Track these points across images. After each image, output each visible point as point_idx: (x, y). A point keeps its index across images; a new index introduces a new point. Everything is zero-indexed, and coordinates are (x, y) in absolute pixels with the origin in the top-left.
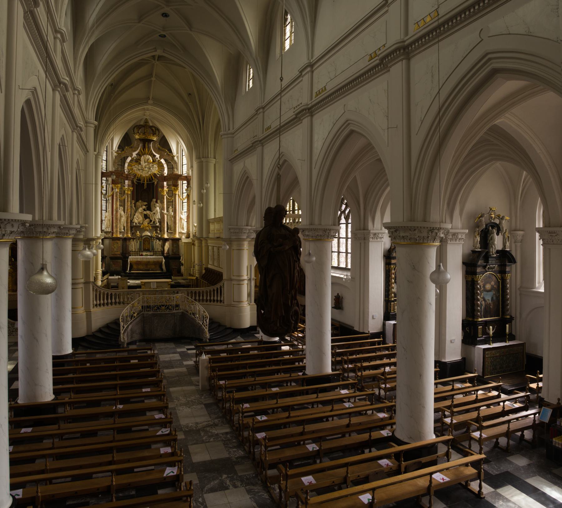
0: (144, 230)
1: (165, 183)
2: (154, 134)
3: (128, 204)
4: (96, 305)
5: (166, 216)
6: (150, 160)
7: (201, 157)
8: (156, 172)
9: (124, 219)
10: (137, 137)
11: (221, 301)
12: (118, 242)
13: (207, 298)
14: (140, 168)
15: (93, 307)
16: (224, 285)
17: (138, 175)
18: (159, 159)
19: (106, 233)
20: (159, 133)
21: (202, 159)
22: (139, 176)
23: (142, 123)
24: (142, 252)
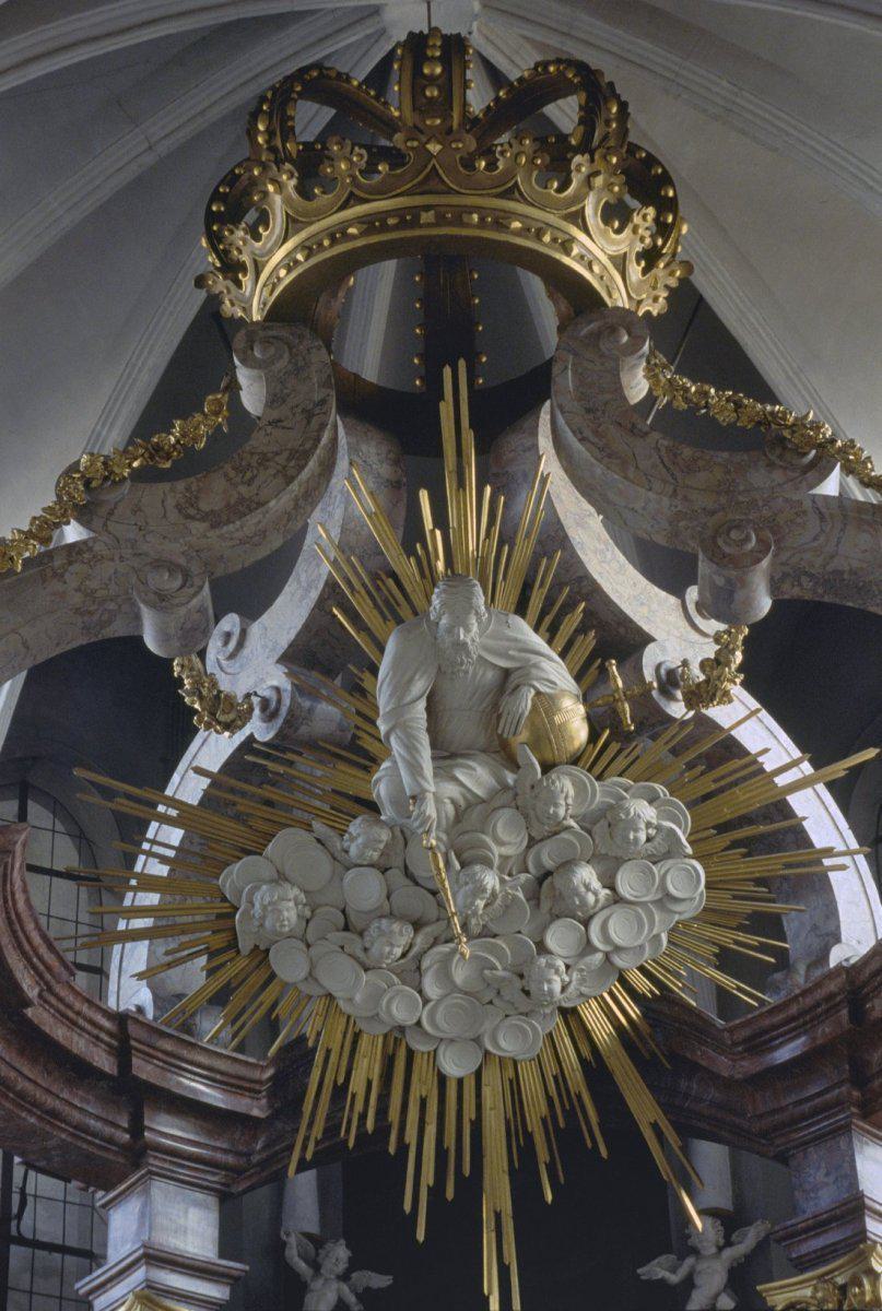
6: (546, 704)
14: (366, 890)
17: (334, 1039)
22: (367, 1068)
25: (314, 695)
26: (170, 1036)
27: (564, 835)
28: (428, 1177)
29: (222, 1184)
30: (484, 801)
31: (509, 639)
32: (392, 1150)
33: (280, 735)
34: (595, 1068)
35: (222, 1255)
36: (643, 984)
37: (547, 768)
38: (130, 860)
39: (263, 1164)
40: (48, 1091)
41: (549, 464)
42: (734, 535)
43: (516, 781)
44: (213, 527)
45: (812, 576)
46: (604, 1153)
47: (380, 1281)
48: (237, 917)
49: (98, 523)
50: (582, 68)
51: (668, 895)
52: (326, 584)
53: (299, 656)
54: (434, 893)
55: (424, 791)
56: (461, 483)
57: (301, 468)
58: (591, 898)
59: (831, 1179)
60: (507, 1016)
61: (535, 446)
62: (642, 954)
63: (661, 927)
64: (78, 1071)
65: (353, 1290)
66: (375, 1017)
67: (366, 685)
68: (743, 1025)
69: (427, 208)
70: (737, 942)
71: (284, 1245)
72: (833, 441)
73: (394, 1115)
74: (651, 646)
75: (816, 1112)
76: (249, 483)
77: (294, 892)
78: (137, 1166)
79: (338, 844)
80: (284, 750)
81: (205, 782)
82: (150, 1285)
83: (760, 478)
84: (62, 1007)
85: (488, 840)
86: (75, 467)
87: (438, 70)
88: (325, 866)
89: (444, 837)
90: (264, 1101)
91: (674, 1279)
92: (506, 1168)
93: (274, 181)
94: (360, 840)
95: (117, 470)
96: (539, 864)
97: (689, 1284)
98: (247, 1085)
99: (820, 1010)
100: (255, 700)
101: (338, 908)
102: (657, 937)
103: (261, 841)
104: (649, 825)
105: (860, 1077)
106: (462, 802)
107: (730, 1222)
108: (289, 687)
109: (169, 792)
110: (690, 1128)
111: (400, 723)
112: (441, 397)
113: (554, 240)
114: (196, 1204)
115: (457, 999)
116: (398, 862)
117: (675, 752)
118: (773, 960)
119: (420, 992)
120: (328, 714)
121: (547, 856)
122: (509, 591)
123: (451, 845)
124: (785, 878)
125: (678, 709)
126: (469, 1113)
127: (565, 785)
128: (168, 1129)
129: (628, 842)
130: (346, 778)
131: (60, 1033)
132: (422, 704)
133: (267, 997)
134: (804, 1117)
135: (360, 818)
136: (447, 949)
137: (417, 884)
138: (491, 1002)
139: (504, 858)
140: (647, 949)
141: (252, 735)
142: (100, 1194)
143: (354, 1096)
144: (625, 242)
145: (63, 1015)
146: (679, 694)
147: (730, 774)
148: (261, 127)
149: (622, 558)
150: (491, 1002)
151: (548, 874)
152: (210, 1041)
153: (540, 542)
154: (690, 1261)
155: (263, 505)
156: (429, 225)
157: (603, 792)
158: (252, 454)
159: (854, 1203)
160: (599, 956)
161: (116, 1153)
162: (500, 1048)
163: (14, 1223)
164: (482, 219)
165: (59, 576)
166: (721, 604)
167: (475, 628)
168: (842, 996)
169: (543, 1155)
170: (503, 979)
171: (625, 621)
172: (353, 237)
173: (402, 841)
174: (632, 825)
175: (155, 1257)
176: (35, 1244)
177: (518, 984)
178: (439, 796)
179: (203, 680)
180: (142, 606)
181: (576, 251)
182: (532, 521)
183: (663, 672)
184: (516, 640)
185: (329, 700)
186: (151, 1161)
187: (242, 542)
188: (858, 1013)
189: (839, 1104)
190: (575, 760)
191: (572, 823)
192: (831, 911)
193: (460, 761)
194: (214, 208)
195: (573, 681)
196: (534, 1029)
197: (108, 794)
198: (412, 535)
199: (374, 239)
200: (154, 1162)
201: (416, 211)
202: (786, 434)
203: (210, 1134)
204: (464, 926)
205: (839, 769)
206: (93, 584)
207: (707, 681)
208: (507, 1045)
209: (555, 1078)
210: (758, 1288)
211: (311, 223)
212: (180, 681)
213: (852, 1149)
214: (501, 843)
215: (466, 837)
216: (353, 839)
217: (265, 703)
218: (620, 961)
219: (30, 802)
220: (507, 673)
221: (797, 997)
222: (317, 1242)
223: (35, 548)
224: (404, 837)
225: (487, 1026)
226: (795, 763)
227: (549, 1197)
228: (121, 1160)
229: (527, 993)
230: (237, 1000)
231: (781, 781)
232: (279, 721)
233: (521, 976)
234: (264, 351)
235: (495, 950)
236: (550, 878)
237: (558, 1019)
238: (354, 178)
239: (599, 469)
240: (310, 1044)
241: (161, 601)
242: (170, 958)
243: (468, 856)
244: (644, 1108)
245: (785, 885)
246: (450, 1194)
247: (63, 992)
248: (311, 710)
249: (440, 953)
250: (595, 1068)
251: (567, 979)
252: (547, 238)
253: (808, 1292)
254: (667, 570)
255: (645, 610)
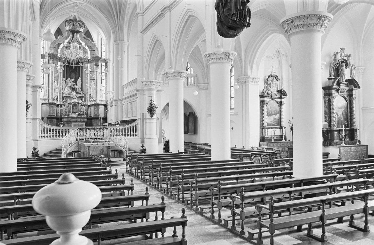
0: (72, 98)
2: (81, 26)
3: (60, 80)
4: (41, 137)
5: (89, 89)
7: (118, 40)
8: (82, 57)
9: (57, 90)
10: (68, 28)
11: (136, 135)
12: (53, 106)
13: (125, 134)
14: (70, 53)
15: (39, 138)
16: (138, 123)
18: (84, 46)
19: (44, 99)
20: (85, 26)
21: (119, 42)
22: (69, 59)
23: (72, 18)
24: (71, 114)
120: (69, 45)
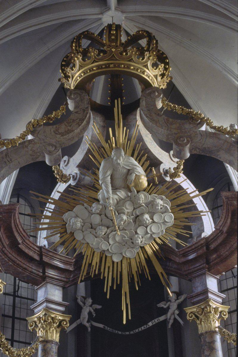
1: (212, 283)
6: (138, 177)
14: (96, 219)
17: (89, 253)
22: (96, 260)
25: (85, 175)
26: (52, 252)
27: (142, 207)
28: (110, 284)
29: (63, 285)
30: (123, 199)
31: (130, 162)
32: (102, 278)
33: (77, 184)
34: (148, 260)
35: (63, 301)
36: (159, 241)
37: (138, 192)
38: (42, 212)
39: (73, 281)
40: (24, 264)
41: (139, 122)
42: (181, 139)
43: (131, 195)
44: (62, 136)
45: (199, 149)
46: (150, 279)
47: (99, 307)
48: (67, 225)
49: (35, 135)
50: (147, 32)
51: (165, 221)
52: (88, 149)
53: (81, 166)
54: (112, 220)
55: (110, 197)
56: (119, 127)
57: (82, 123)
58: (148, 222)
59: (201, 285)
60: (128, 248)
61: (136, 118)
62: (159, 234)
63: (163, 228)
64: (31, 259)
65: (93, 309)
66: (98, 248)
67: (97, 173)
68: (182, 251)
69: (112, 64)
70: (181, 232)
71: (77, 299)
72: (204, 118)
73: (102, 270)
74: (162, 164)
75: (198, 270)
76: (70, 126)
77: (80, 220)
78: (44, 281)
79: (90, 209)
80: (78, 187)
81: (60, 194)
82: (47, 307)
83: (187, 126)
84: (27, 245)
85: (124, 208)
86: (30, 122)
87: (114, 32)
88: (87, 214)
89: (114, 207)
90: (73, 267)
91: (165, 307)
92: (128, 282)
93: (77, 57)
94: (95, 208)
95: (40, 123)
96: (136, 214)
97: (168, 308)
98: (69, 263)
99: (199, 247)
100: (71, 176)
101: (89, 223)
102: (163, 230)
103: (72, 208)
104: (161, 205)
105: (208, 262)
106: (118, 200)
107: (178, 294)
108: (79, 173)
109: (51, 196)
110: (169, 274)
111: (104, 181)
112: (114, 106)
113: (141, 71)
114: (58, 290)
115: (117, 244)
116: (104, 213)
117: (167, 188)
118: (189, 236)
119: (108, 243)
120: (88, 179)
121: (138, 212)
122: (130, 151)
123: (116, 209)
124: (192, 217)
125: (168, 179)
126: (119, 270)
127: (142, 196)
128: (51, 273)
129: (156, 208)
130: (92, 194)
131: (26, 251)
132: (109, 177)
133: (74, 243)
134: (195, 271)
135: (95, 204)
136: (115, 233)
137: (108, 218)
138: (124, 245)
139: (128, 212)
140: (160, 233)
141: (70, 184)
142: (36, 287)
143: (93, 266)
144: (157, 72)
145: (28, 247)
146: (168, 175)
147: (180, 194)
148: (74, 45)
149: (156, 144)
150: (124, 245)
151: (138, 216)
152: (60, 253)
153: (137, 140)
154: (169, 303)
155: (73, 131)
156: (112, 67)
157: (151, 198)
158: (71, 119)
159: (206, 290)
160: (149, 235)
161: (39, 278)
162: (126, 255)
163: (16, 293)
164: (124, 66)
165: (27, 147)
166: (178, 155)
167: (122, 160)
168: (204, 244)
169: (136, 279)
170: (128, 240)
171: (156, 159)
172: (95, 70)
173: (105, 208)
174: (157, 205)
175: (48, 301)
176: (21, 297)
177: (131, 241)
178: (113, 198)
179: (59, 171)
180: (45, 154)
181: (146, 74)
182: (135, 135)
183: (165, 170)
184: (131, 163)
185: (88, 176)
186: (47, 280)
187: (68, 140)
188: (208, 248)
189: (203, 268)
190: (144, 190)
191: (143, 204)
192: (202, 225)
193: (118, 190)
194: (63, 63)
195: (144, 172)
196: (134, 251)
197: (38, 197)
198: (108, 138)
199: (99, 71)
200: (48, 280)
201: (109, 64)
202: (193, 116)
203: (60, 274)
204: (119, 228)
205: (205, 193)
206: (34, 149)
207: (175, 172)
208: (128, 255)
209: (139, 262)
210: (184, 309)
211: (85, 67)
212: (54, 172)
213: (206, 278)
214: (127, 209)
215: (120, 207)
216: (93, 208)
217: (73, 177)
218: (154, 236)
219: (20, 198)
220: (129, 170)
221: (194, 244)
222: (85, 298)
223: (21, 141)
224: (105, 207)
225: (124, 250)
226: (195, 191)
227: (137, 289)
228: (40, 279)
229: (133, 243)
230: (66, 244)
231: (191, 195)
232: (77, 181)
233: (131, 239)
234: (74, 96)
235: (126, 234)
236: (138, 218)
237: (140, 249)
238: (95, 57)
239: (151, 124)
240: (83, 254)
241: (50, 153)
242: (51, 234)
243: (120, 212)
244: (159, 269)
245: (192, 219)
246: (115, 288)
247: (27, 242)
248: (84, 178)
249: (113, 234)
250: (148, 260)
251: (142, 240)
252: (139, 71)
253: (195, 310)
254: (166, 147)
255: (161, 156)
